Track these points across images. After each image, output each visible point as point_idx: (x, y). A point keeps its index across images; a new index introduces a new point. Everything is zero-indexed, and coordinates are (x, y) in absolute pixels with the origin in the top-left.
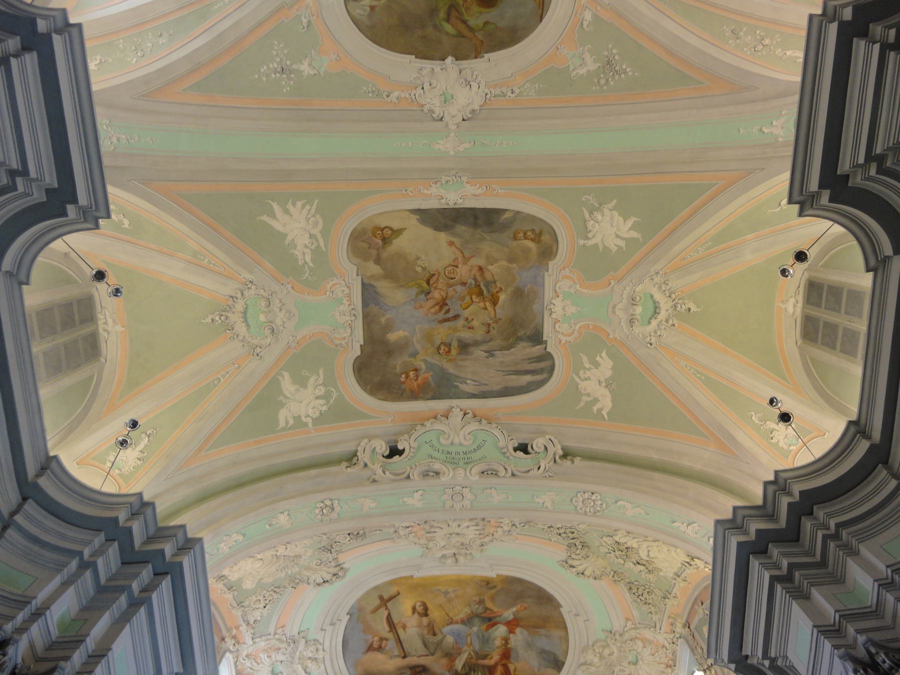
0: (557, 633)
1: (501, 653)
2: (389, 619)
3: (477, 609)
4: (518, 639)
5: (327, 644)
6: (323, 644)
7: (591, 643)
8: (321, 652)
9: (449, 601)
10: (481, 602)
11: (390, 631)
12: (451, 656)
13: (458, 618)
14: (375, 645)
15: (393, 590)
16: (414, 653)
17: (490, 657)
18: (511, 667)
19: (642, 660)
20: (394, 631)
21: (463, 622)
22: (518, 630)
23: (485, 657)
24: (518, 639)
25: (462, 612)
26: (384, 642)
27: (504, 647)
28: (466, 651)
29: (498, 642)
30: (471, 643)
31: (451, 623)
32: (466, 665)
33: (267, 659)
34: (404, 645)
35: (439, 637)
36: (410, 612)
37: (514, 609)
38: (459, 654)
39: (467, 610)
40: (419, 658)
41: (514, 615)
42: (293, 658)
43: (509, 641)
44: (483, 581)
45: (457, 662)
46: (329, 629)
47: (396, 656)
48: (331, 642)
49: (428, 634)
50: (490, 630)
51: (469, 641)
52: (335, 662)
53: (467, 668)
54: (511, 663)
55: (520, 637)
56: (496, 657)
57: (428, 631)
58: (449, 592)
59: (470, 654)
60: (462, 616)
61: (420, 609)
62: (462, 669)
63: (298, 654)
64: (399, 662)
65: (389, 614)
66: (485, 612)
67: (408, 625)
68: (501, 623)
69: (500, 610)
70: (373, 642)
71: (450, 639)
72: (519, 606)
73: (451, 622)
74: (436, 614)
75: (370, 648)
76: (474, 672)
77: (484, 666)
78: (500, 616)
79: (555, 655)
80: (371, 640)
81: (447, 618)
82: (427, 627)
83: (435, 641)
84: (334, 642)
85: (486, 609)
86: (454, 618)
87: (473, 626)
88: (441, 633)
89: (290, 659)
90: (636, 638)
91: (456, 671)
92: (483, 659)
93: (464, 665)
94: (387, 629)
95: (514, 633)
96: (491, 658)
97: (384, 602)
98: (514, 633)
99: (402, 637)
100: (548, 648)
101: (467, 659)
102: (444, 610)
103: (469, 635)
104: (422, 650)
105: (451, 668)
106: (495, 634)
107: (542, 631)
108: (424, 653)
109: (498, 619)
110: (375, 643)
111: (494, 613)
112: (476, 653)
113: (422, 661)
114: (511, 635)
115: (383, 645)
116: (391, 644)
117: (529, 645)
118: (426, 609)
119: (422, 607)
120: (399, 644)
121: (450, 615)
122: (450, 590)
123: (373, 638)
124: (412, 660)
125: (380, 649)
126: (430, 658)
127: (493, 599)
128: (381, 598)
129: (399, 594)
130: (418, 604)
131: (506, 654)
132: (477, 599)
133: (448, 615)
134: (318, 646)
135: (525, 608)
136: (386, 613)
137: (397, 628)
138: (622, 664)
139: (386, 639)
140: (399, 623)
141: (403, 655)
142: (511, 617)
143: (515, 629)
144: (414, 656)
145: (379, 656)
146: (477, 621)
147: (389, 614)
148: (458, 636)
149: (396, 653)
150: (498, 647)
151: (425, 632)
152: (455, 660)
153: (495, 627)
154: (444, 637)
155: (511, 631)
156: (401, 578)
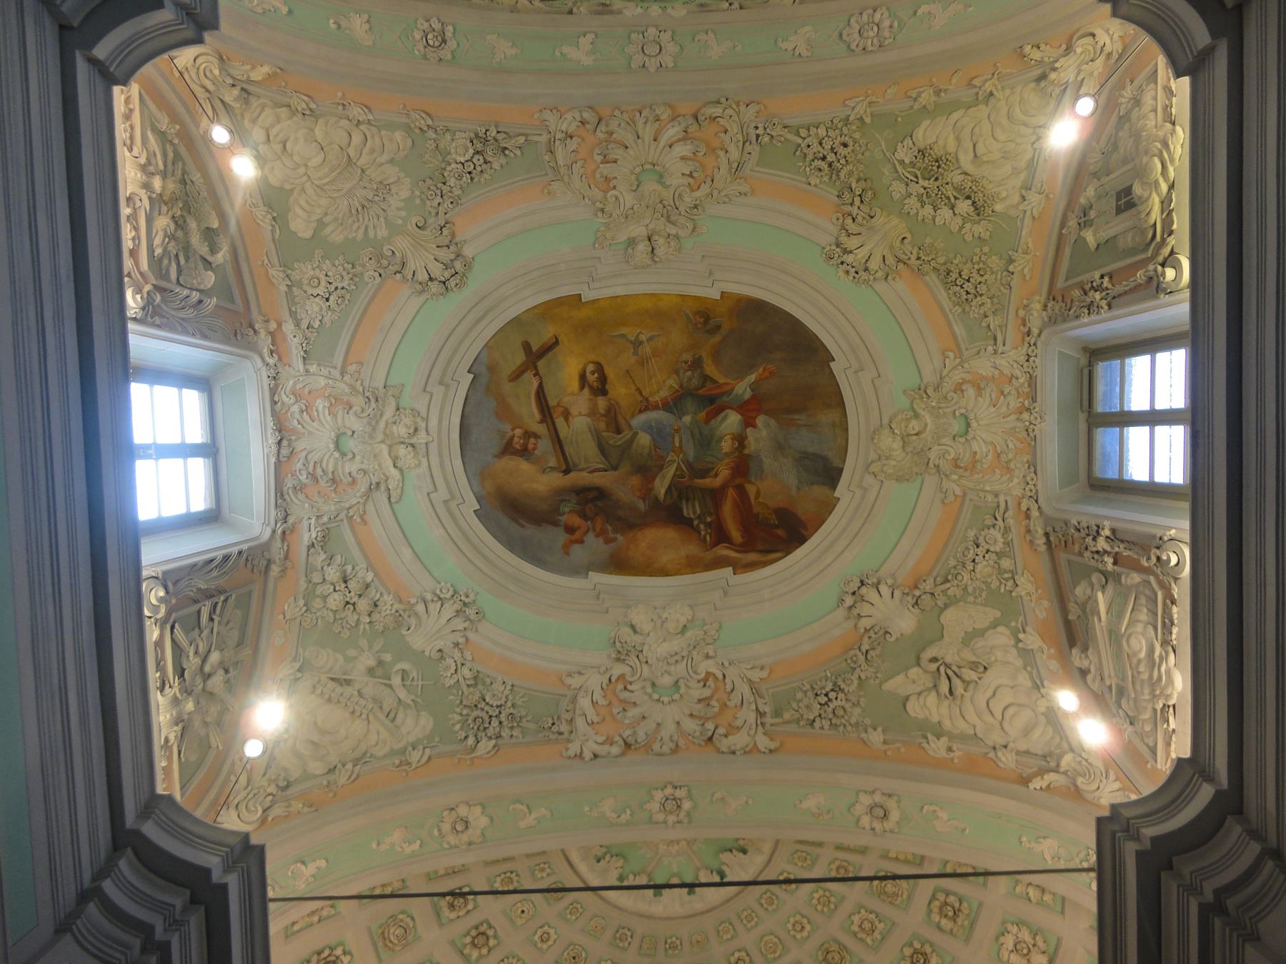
0: (827, 417)
1: (733, 464)
2: (541, 395)
3: (690, 379)
4: (762, 435)
5: (433, 422)
6: (427, 420)
7: (885, 421)
8: (422, 434)
9: (642, 363)
10: (696, 364)
11: (541, 422)
12: (647, 471)
13: (656, 398)
14: (517, 443)
15: (547, 332)
16: (583, 465)
17: (713, 472)
18: (751, 490)
19: (977, 421)
20: (549, 419)
21: (666, 406)
22: (760, 420)
23: (705, 473)
24: (762, 435)
25: (663, 385)
26: (532, 440)
27: (737, 454)
28: (674, 461)
29: (726, 445)
30: (681, 447)
31: (646, 409)
32: (673, 489)
33: (328, 418)
34: (566, 449)
35: (627, 435)
36: (575, 384)
37: (752, 377)
38: (661, 468)
39: (672, 382)
40: (591, 475)
41: (753, 390)
42: (374, 429)
43: (746, 442)
44: (698, 313)
45: (657, 481)
46: (438, 392)
47: (552, 469)
48: (440, 421)
49: (607, 430)
50: (713, 422)
51: (677, 445)
52: (447, 462)
53: (675, 494)
54: (750, 482)
55: (764, 433)
56: (724, 473)
57: (608, 425)
58: (641, 343)
59: (679, 468)
60: (664, 393)
61: (592, 378)
62: (665, 495)
63: (382, 425)
64: (557, 480)
65: (541, 387)
66: (703, 386)
67: (574, 411)
68: (731, 408)
69: (728, 381)
70: (512, 437)
71: (644, 439)
72: (761, 370)
73: (647, 406)
74: (620, 391)
75: (508, 449)
76: (688, 500)
77: (704, 490)
78: (730, 392)
79: (825, 459)
80: (511, 433)
81: (640, 398)
82: (605, 416)
83: (619, 443)
84: (445, 423)
85: (706, 378)
86: (650, 399)
87: (684, 414)
88: (630, 427)
89: (368, 429)
90: (964, 381)
91: (656, 499)
92: (704, 477)
93: (670, 486)
94: (537, 416)
95: (754, 426)
96: (716, 475)
97: (535, 356)
98: (754, 426)
99: (562, 435)
100: (810, 450)
101: (674, 475)
102: (634, 383)
103: (677, 431)
104: (597, 460)
105: (647, 492)
106: (723, 426)
107: (802, 418)
108: (602, 466)
109: (725, 399)
110: (516, 439)
111: (720, 386)
112: (690, 466)
113: (598, 479)
114: (749, 430)
115: (530, 446)
116: (544, 446)
117: (780, 448)
118: (603, 379)
119: (596, 375)
120: (558, 446)
121: (644, 394)
122: (643, 338)
123: (513, 430)
124: (580, 478)
125: (524, 452)
126: (612, 475)
127: (716, 356)
128: (527, 347)
129: (556, 342)
130: (591, 368)
131: (743, 466)
132: (687, 357)
133: (641, 394)
134: (418, 420)
135: (772, 373)
136: (535, 383)
137: (554, 416)
138: (943, 441)
139: (536, 436)
140: (558, 405)
141: (564, 467)
142: (748, 395)
143: (756, 417)
144: (582, 470)
145: (524, 466)
146: (689, 405)
147: (541, 387)
148: (658, 433)
149: (553, 463)
150: (727, 454)
151: (602, 425)
152: (654, 478)
153: (723, 414)
154: (636, 434)
155: (749, 423)
156: (559, 302)
